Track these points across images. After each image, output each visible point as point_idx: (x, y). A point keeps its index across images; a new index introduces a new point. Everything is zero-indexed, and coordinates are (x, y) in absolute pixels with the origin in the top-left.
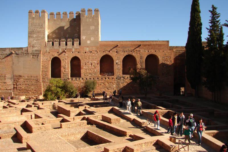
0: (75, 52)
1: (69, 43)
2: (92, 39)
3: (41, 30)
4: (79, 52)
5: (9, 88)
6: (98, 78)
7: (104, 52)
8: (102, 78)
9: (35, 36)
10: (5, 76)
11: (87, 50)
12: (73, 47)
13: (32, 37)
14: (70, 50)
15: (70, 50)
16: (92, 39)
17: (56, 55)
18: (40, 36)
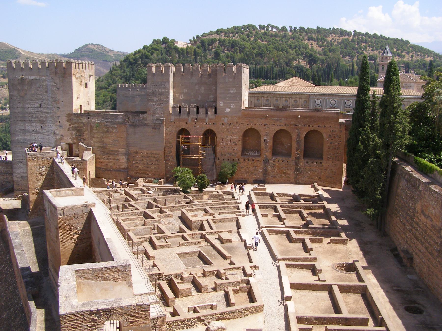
0: (209, 124)
1: (201, 111)
2: (233, 106)
3: (163, 92)
4: (214, 123)
5: (123, 167)
6: (239, 160)
7: (247, 124)
8: (244, 160)
9: (155, 99)
10: (117, 151)
11: (226, 120)
12: (206, 117)
13: (152, 101)
14: (203, 120)
15: (203, 120)
16: (232, 106)
17: (183, 127)
18: (162, 99)
